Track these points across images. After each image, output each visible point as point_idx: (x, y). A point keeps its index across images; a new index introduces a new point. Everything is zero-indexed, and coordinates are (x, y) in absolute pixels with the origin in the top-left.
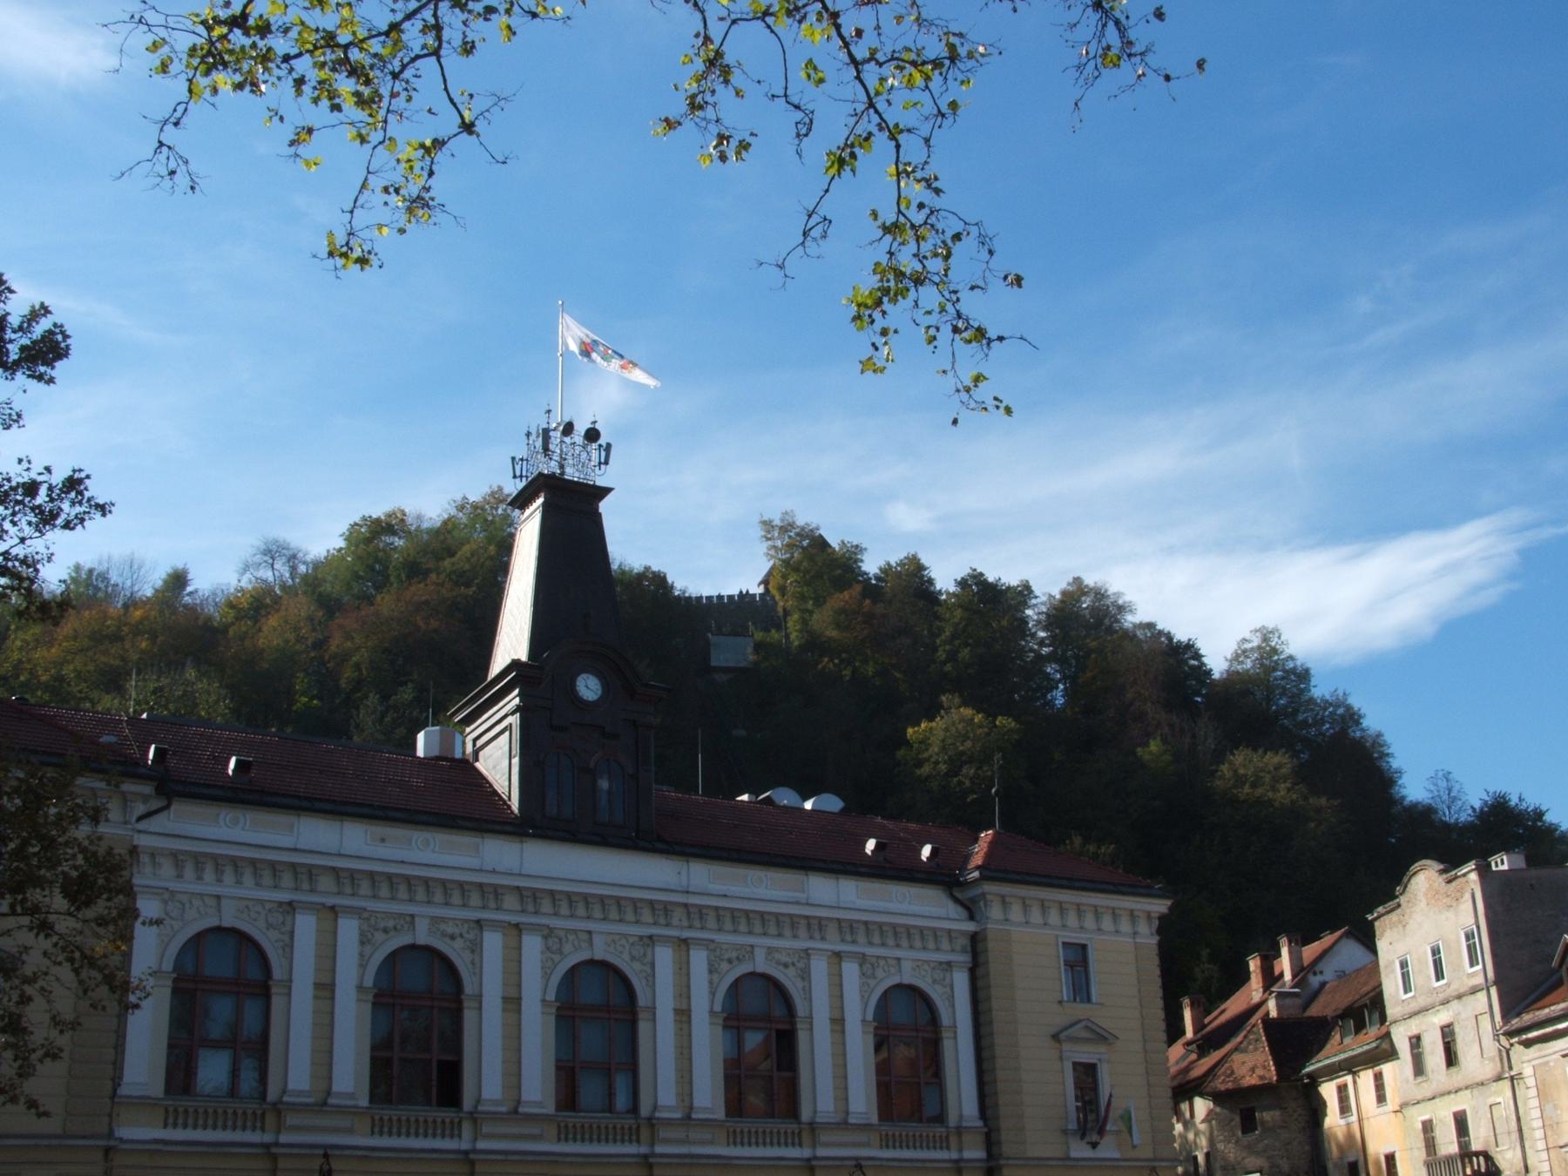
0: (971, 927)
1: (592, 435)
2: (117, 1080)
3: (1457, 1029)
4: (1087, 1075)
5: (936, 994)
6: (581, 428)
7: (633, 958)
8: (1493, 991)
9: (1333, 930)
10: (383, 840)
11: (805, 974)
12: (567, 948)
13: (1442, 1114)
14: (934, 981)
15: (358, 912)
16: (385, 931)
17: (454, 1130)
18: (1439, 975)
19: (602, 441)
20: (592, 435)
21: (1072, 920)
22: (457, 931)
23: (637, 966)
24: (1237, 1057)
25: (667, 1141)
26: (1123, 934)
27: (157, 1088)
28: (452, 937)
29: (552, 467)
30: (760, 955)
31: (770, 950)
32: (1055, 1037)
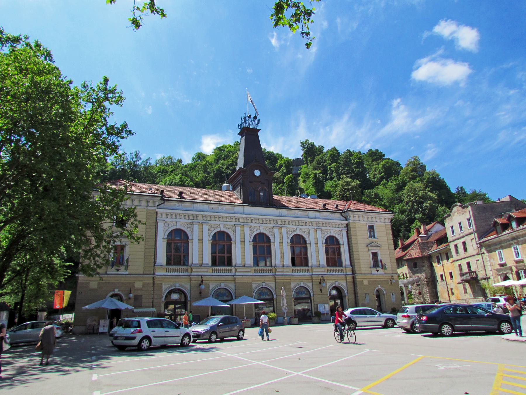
0: (346, 222)
1: (255, 118)
2: (155, 263)
3: (466, 242)
4: (375, 255)
5: (339, 237)
6: (252, 116)
8: (476, 234)
9: (433, 221)
12: (255, 230)
13: (464, 263)
18: (461, 230)
19: (258, 119)
20: (255, 118)
21: (370, 219)
23: (271, 233)
24: (412, 251)
25: (279, 272)
26: (383, 221)
29: (247, 126)
30: (298, 230)
32: (367, 246)
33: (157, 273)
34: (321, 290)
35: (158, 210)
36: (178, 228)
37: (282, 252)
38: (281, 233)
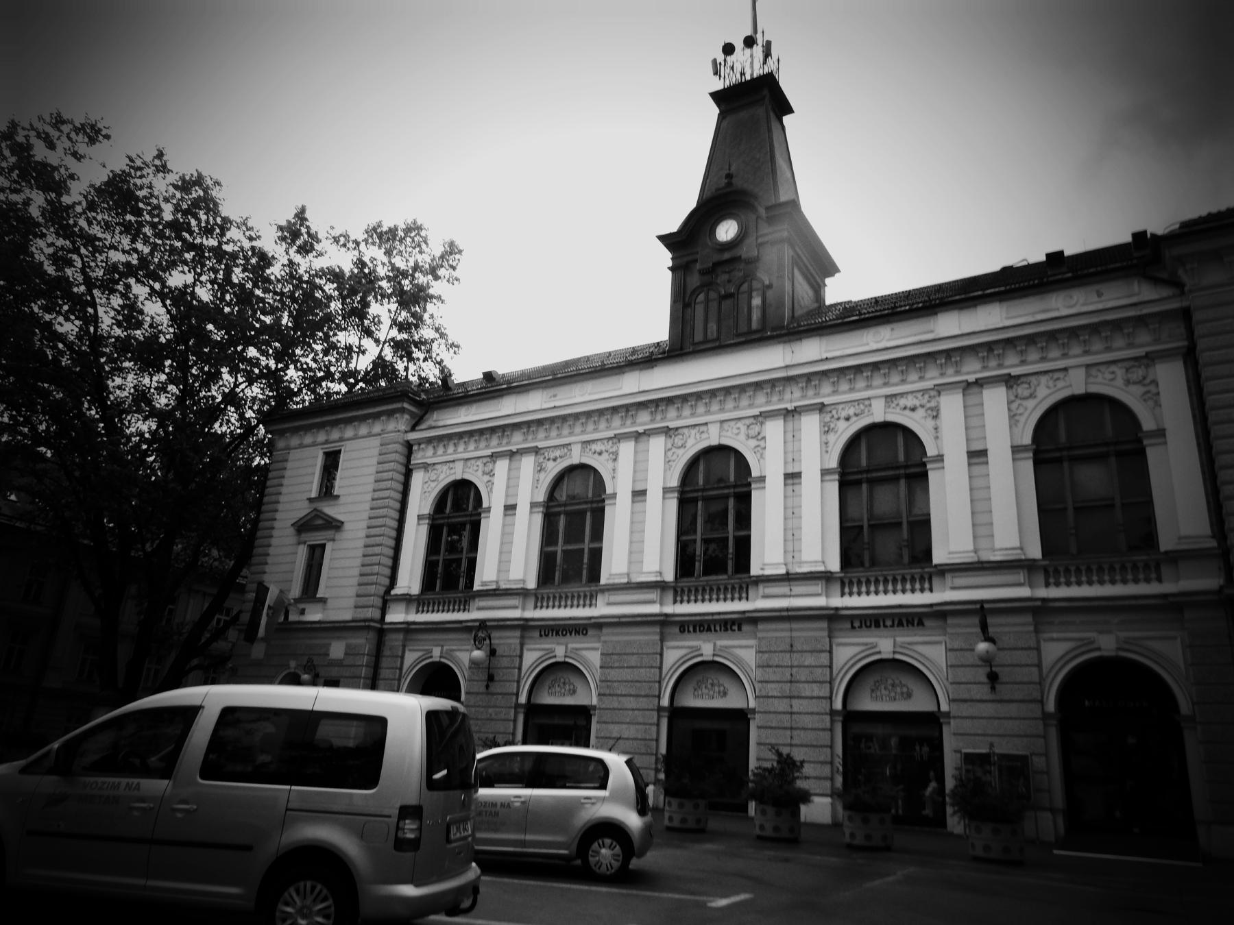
5: (1130, 397)
7: (748, 437)
10: (555, 396)
11: (935, 414)
14: (1128, 382)
15: (536, 451)
16: (555, 460)
17: (590, 599)
22: (603, 448)
23: (753, 443)
27: (415, 589)
28: (600, 454)
31: (890, 398)
33: (390, 618)
34: (993, 678)
35: (413, 436)
36: (459, 477)
37: (792, 514)
38: (791, 438)
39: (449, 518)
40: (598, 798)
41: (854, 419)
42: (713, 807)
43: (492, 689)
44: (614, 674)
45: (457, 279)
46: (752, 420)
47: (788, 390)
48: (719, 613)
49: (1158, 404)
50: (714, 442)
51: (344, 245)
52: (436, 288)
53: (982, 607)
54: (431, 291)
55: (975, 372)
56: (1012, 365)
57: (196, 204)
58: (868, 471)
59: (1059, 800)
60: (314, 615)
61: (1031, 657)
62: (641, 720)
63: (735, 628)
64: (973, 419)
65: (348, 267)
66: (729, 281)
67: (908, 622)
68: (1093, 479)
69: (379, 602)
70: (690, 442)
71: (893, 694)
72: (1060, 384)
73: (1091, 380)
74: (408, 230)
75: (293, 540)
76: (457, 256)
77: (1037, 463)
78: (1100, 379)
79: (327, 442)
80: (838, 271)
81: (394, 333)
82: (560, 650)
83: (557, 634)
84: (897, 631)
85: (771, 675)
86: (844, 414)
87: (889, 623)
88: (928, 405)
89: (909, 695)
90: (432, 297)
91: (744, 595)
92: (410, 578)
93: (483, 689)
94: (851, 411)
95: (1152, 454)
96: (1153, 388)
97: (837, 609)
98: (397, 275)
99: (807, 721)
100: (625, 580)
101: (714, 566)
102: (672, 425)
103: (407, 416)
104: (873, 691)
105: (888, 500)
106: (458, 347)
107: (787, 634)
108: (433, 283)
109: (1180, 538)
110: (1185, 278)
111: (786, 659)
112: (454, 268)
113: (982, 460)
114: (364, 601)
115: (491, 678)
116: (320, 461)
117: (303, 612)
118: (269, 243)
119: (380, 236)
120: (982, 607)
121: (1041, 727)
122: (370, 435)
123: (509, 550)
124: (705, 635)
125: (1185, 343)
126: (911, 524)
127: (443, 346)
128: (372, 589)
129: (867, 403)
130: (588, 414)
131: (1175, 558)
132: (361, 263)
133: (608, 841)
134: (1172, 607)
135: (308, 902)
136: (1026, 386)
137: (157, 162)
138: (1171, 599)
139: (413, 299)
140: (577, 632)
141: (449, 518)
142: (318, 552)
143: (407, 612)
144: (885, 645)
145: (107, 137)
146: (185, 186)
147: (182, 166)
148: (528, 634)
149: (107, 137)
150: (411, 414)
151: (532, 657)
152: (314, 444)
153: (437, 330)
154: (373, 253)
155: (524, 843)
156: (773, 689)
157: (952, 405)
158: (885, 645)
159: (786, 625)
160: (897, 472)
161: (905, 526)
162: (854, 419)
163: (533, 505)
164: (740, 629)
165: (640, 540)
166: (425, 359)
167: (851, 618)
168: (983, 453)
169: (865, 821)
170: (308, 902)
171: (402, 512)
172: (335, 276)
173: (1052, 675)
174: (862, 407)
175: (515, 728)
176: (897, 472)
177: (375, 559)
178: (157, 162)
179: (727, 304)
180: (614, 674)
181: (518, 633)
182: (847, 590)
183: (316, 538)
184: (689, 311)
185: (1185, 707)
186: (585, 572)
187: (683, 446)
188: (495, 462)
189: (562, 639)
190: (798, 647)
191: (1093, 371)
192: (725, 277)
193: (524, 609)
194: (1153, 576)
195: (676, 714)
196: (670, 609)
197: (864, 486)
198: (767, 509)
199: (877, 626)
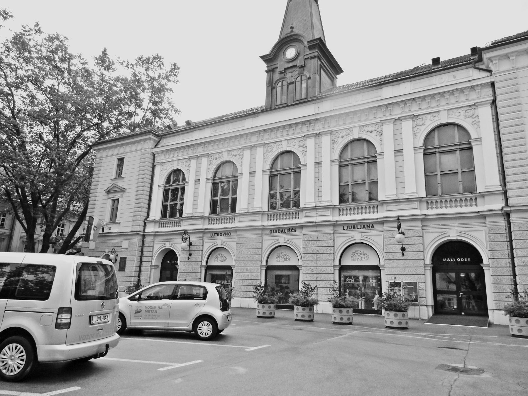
10: (216, 131)
14: (466, 117)
15: (208, 155)
22: (237, 153)
23: (302, 149)
33: (147, 230)
34: (403, 249)
35: (155, 150)
37: (318, 180)
38: (318, 147)
39: (171, 186)
40: (201, 303)
41: (345, 137)
42: (277, 307)
43: (190, 260)
44: (242, 252)
45: (178, 81)
46: (301, 139)
47: (317, 125)
48: (286, 224)
49: (478, 127)
50: (285, 149)
51: (127, 66)
52: (170, 85)
53: (398, 219)
54: (167, 87)
55: (398, 115)
56: (415, 109)
57: (57, 49)
58: (351, 160)
59: (430, 301)
60: (115, 229)
61: (420, 240)
62: (253, 271)
63: (293, 231)
64: (397, 135)
65: (129, 77)
66: (292, 76)
67: (367, 226)
68: (451, 162)
69: (143, 224)
70: (274, 149)
71: (360, 258)
72: (436, 118)
73: (450, 116)
74: (154, 58)
75: (106, 197)
76: (177, 71)
77: (425, 154)
78: (453, 116)
79: (118, 154)
80: (342, 71)
81: (151, 106)
82: (219, 242)
83: (218, 235)
84: (363, 230)
85: (308, 250)
86: (341, 135)
87: (359, 227)
88: (378, 130)
89: (367, 258)
90: (167, 90)
91: (297, 216)
92: (156, 212)
93: (187, 260)
94: (344, 134)
95: (474, 148)
96: (476, 119)
97: (337, 221)
98: (152, 80)
99: (323, 270)
100: (246, 211)
101: (285, 204)
102: (266, 142)
103: (152, 142)
104: (352, 256)
105: (361, 173)
106: (180, 111)
107: (316, 233)
108: (168, 83)
109: (486, 186)
110: (492, 67)
111: (315, 244)
112: (176, 76)
113: (401, 154)
114: (136, 223)
115: (190, 255)
116: (116, 162)
117: (110, 229)
118: (92, 66)
119: (143, 61)
120: (398, 219)
121: (423, 270)
122: (136, 151)
123: (197, 200)
124: (281, 234)
125: (492, 98)
126: (370, 183)
127: (173, 112)
128: (139, 218)
129: (351, 129)
130: (230, 138)
131: (483, 195)
132: (135, 75)
133: (206, 323)
134: (483, 216)
135: (14, 353)
136: (421, 120)
137: (36, 28)
138: (481, 213)
139: (158, 90)
140: (226, 234)
141: (171, 186)
142: (116, 202)
143: (154, 228)
144: (357, 236)
145: (12, 16)
146: (51, 39)
147: (48, 31)
148: (206, 235)
149: (12, 16)
150: (154, 141)
151: (208, 245)
152: (113, 155)
153: (170, 104)
154: (140, 70)
155: (168, 324)
156: (309, 257)
157: (388, 129)
158: (357, 236)
159: (314, 229)
160: (364, 160)
161: (367, 184)
162: (345, 137)
163: (207, 179)
164: (295, 231)
165: (253, 194)
166: (165, 118)
167: (343, 225)
168: (401, 150)
169: (341, 312)
170: (14, 353)
171: (152, 184)
172: (124, 81)
173: (429, 247)
174: (349, 131)
175: (201, 276)
176: (364, 160)
177: (140, 205)
178: (36, 28)
179: (291, 87)
180: (242, 252)
181: (201, 235)
182: (341, 213)
183: (115, 196)
184: (274, 90)
185: (485, 260)
186: (230, 208)
187: (271, 151)
188: (190, 161)
189: (219, 237)
190: (320, 238)
191: (451, 112)
192: (290, 74)
193: (204, 225)
194: (474, 203)
195: (269, 268)
196: (265, 223)
197: (350, 166)
198: (307, 177)
199: (354, 228)
